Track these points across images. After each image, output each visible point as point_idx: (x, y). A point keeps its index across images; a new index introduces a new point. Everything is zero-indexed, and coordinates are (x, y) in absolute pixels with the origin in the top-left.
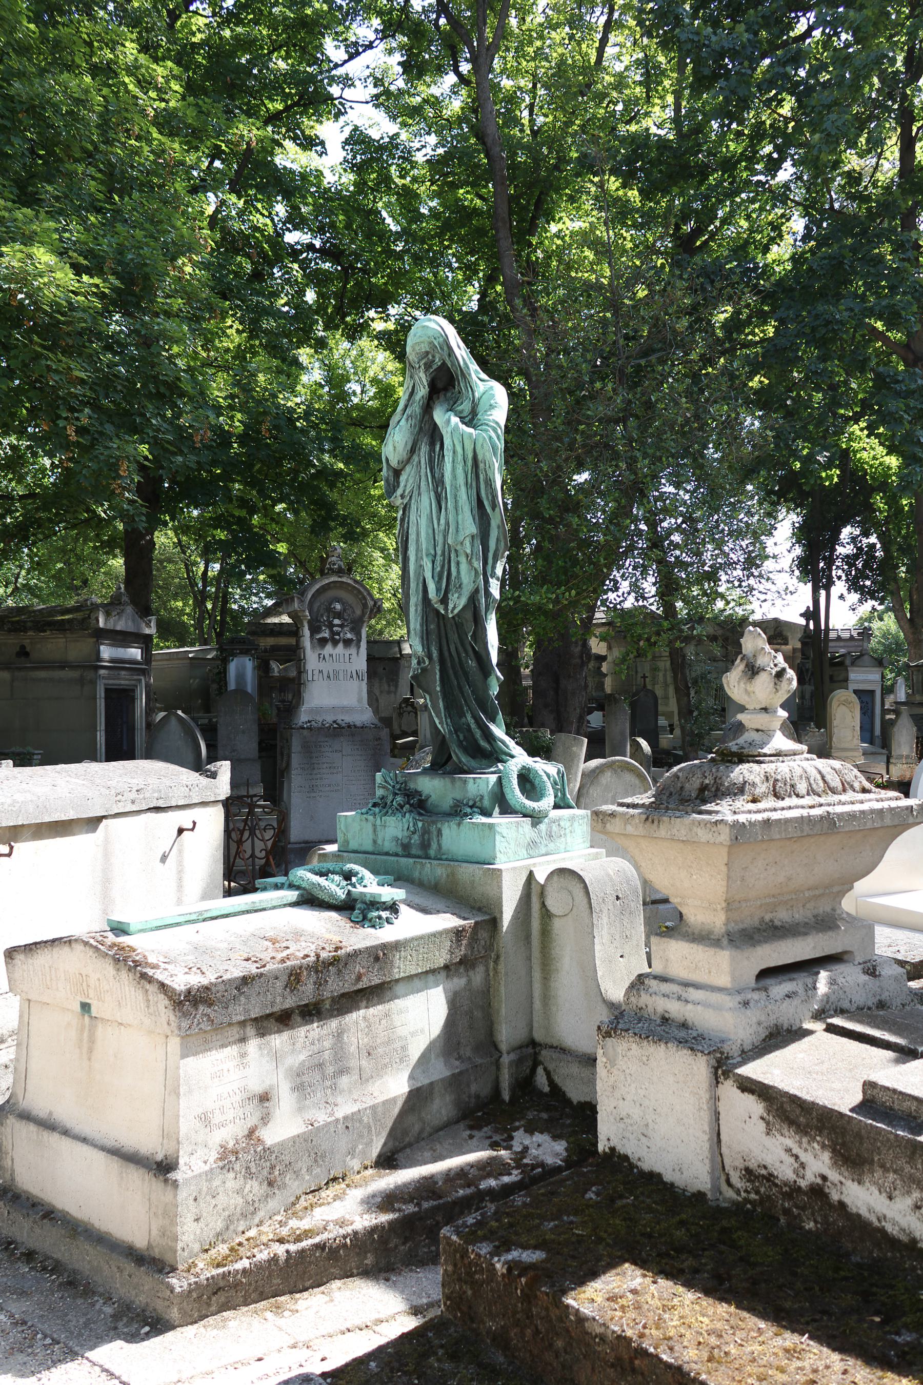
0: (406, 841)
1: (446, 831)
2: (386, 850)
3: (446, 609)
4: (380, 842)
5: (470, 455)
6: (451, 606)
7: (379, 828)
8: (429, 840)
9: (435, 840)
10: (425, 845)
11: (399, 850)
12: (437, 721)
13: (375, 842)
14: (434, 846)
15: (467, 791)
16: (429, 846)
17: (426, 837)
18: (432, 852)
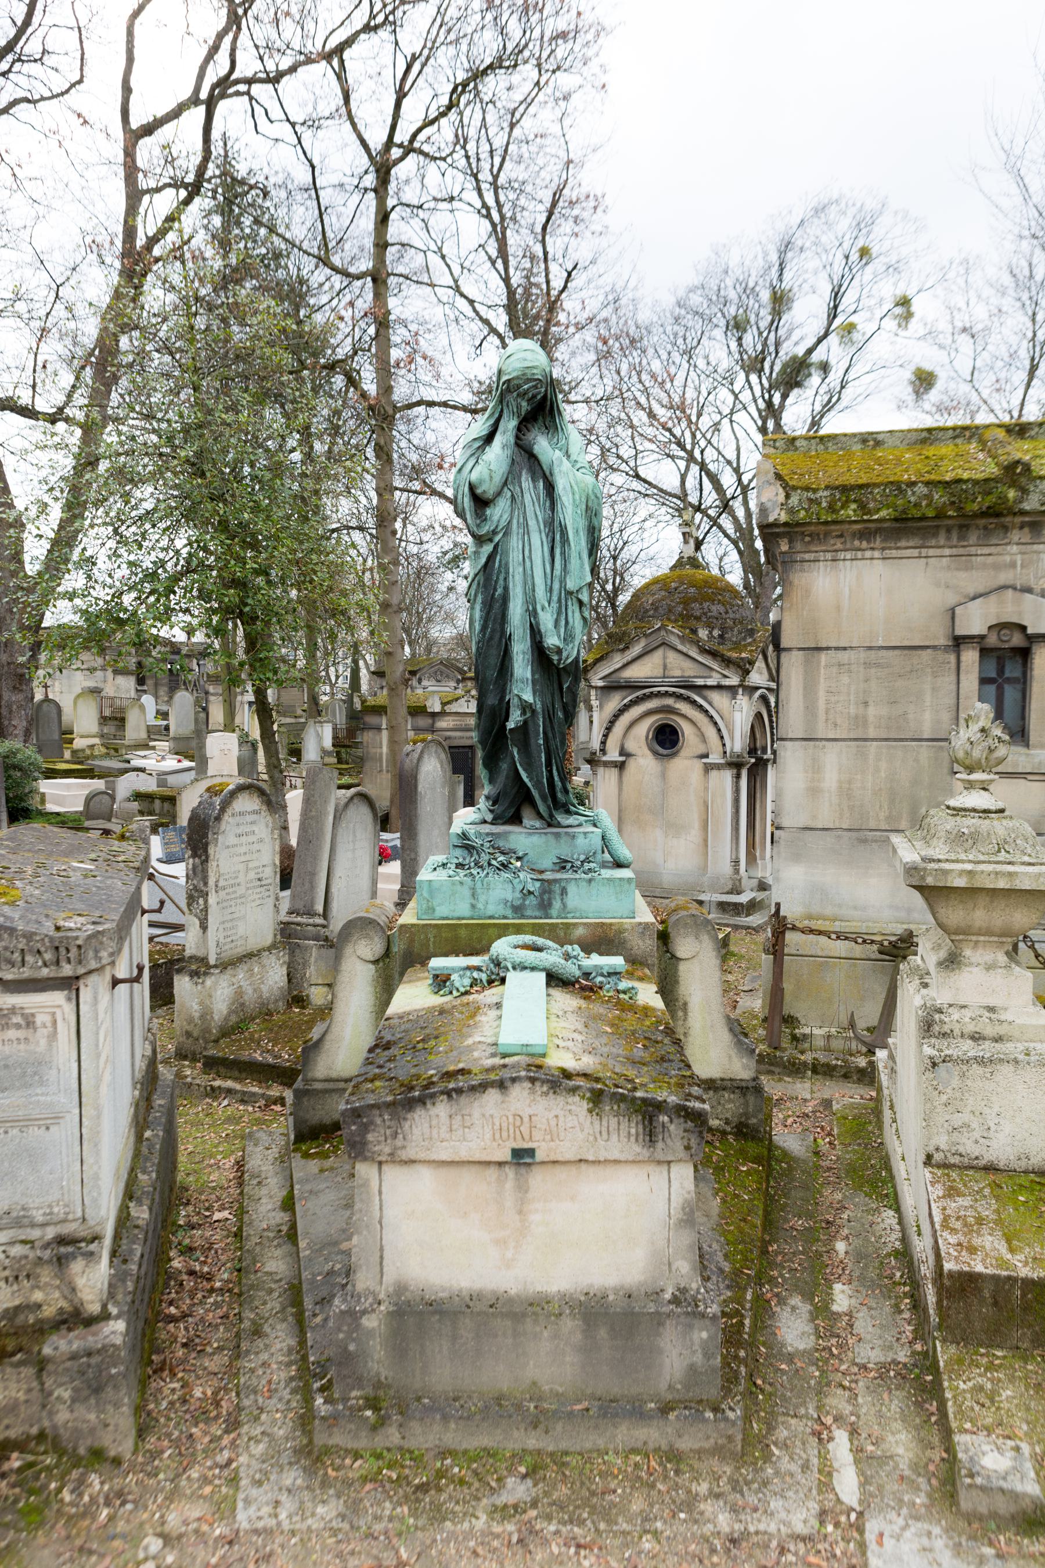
0: (518, 903)
1: (572, 889)
2: (489, 913)
3: (560, 660)
4: (480, 906)
5: (584, 500)
6: (564, 654)
7: (479, 891)
8: (550, 899)
9: (558, 897)
10: (545, 906)
11: (509, 912)
12: (524, 775)
13: (473, 906)
14: (557, 904)
15: (575, 846)
16: (550, 905)
17: (546, 897)
18: (554, 912)
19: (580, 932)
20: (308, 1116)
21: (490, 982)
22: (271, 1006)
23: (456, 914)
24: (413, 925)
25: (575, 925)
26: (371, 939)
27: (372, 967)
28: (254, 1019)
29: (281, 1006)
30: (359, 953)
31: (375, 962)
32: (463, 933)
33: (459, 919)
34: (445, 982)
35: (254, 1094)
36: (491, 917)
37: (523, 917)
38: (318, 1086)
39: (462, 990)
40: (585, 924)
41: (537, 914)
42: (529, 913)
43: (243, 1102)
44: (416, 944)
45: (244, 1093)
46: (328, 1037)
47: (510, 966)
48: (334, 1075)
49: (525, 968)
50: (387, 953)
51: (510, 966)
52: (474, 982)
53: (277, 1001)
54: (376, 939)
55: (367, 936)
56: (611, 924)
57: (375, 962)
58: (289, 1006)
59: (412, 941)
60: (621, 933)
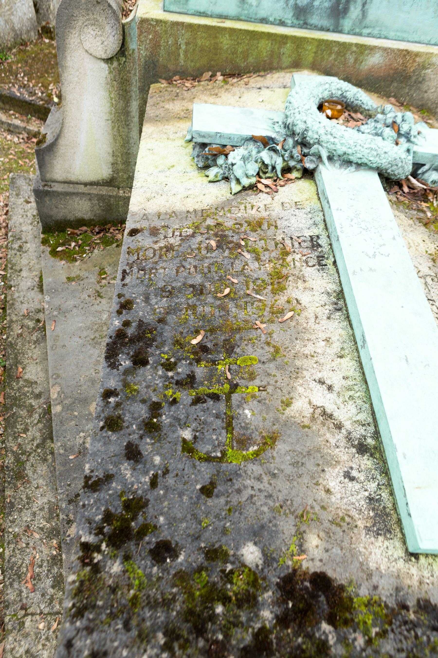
2: (262, 14)
11: (288, 16)
16: (346, 10)
18: (347, 24)
19: (374, 61)
20: (52, 213)
21: (287, 170)
22: (24, 37)
23: (218, 10)
24: (159, 22)
25: (372, 49)
26: (102, 28)
27: (104, 66)
28: (10, 49)
29: (33, 36)
30: (87, 45)
31: (109, 60)
32: (225, 42)
33: (221, 17)
34: (215, 156)
35: (17, 127)
36: (264, 21)
37: (305, 25)
38: (57, 188)
39: (246, 182)
40: (385, 50)
41: (325, 23)
42: (314, 20)
43: (10, 131)
44: (162, 52)
45: (9, 125)
46: (62, 142)
47: (324, 155)
48: (73, 178)
49: (349, 163)
50: (123, 50)
51: (324, 155)
52: (264, 169)
53: (28, 32)
54: (108, 28)
55: (95, 23)
56: (417, 55)
57: (109, 60)
58: (40, 36)
59: (156, 46)
60: (424, 68)
